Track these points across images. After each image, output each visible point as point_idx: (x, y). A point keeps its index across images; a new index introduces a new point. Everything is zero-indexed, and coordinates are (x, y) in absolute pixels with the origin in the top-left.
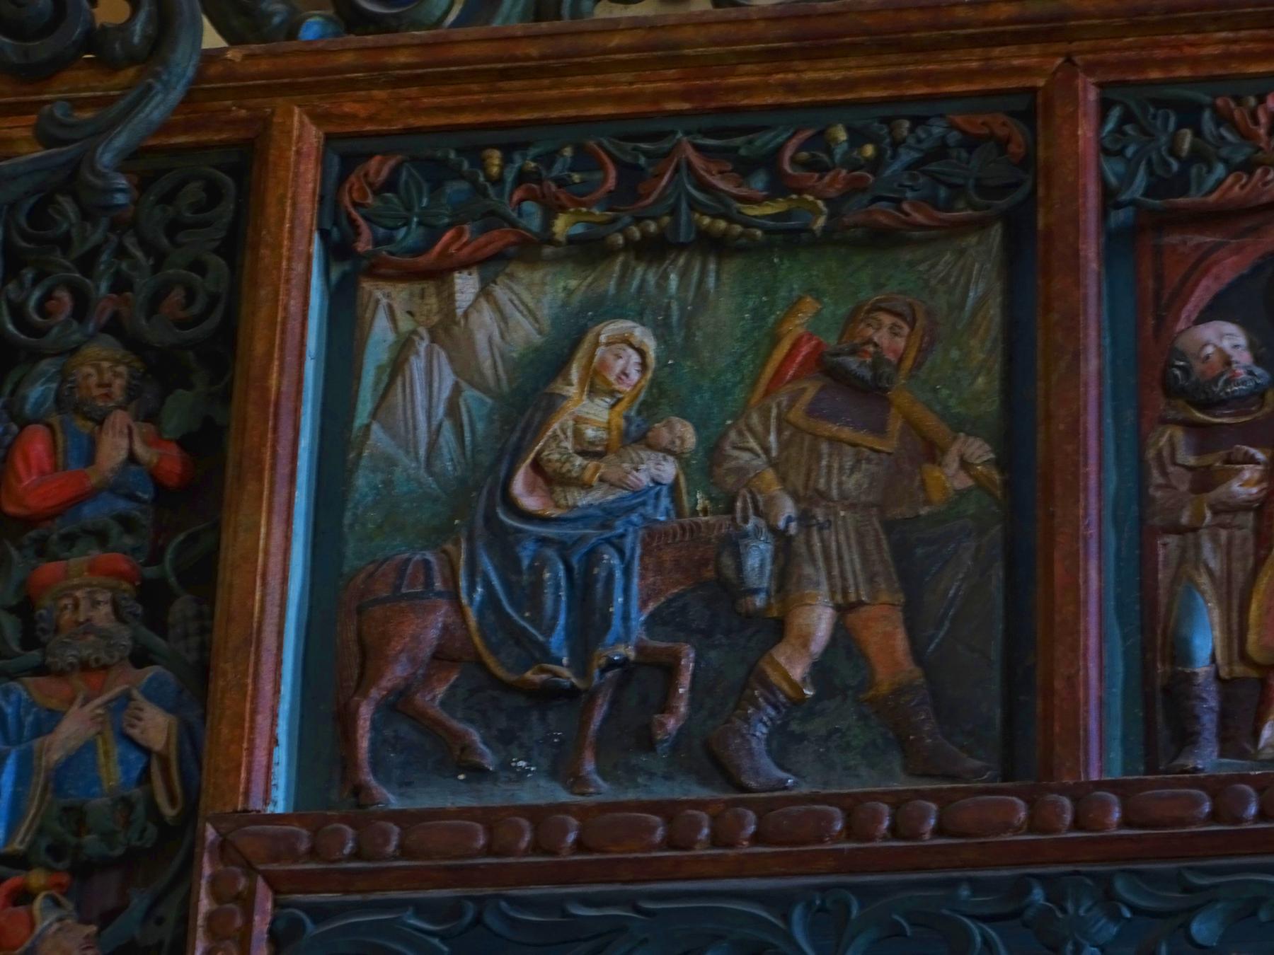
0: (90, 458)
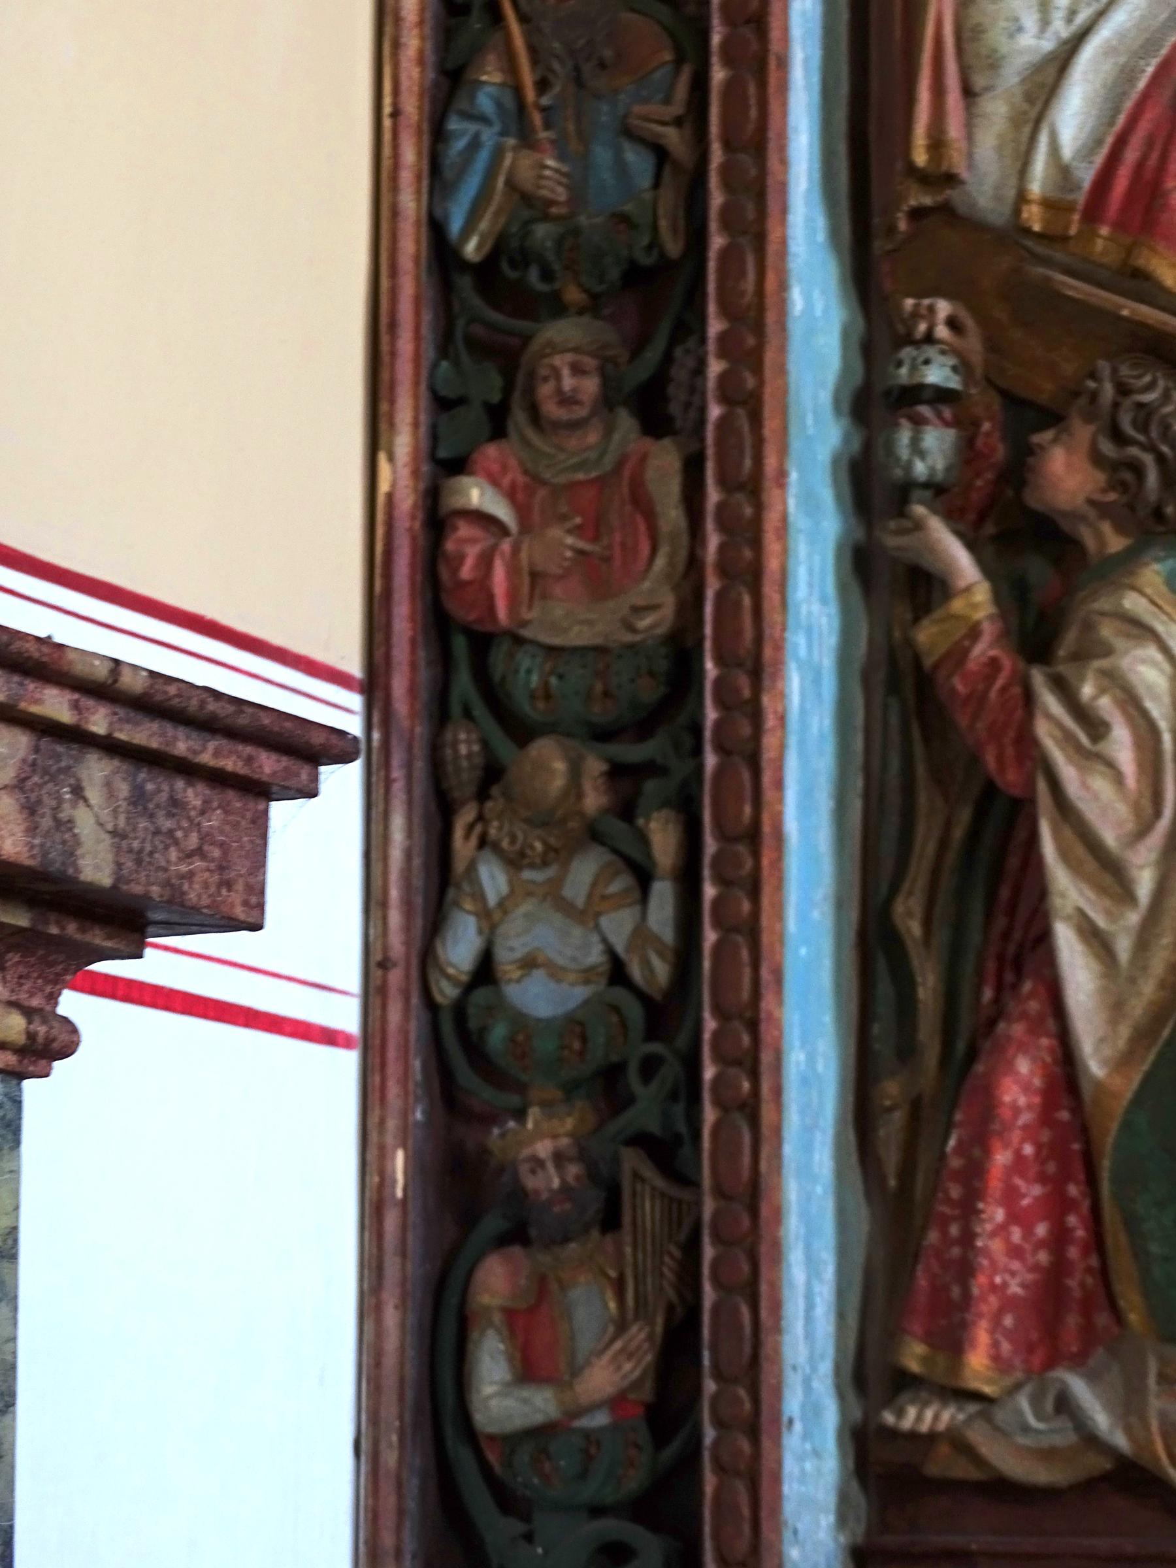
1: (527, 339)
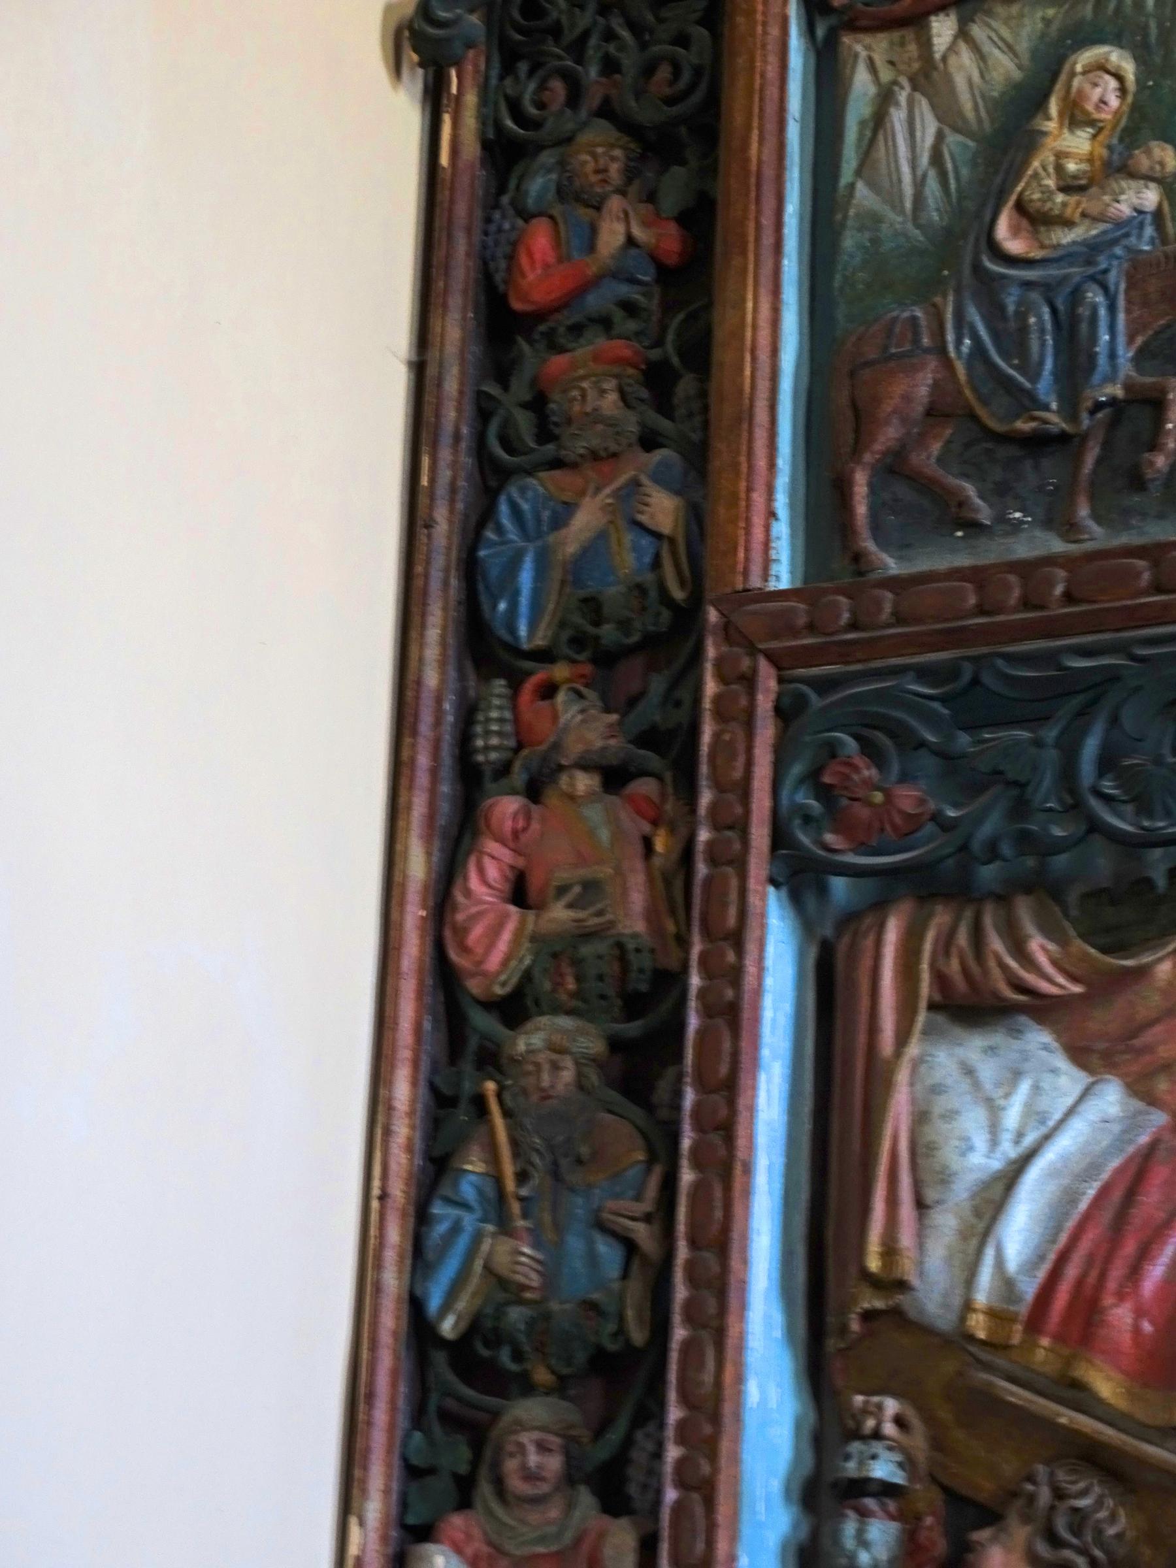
0: (591, 247)
1: (496, 1415)
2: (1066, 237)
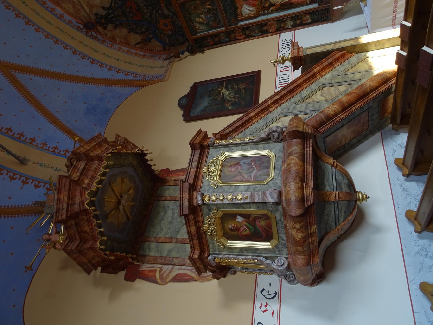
2: (205, 19)
